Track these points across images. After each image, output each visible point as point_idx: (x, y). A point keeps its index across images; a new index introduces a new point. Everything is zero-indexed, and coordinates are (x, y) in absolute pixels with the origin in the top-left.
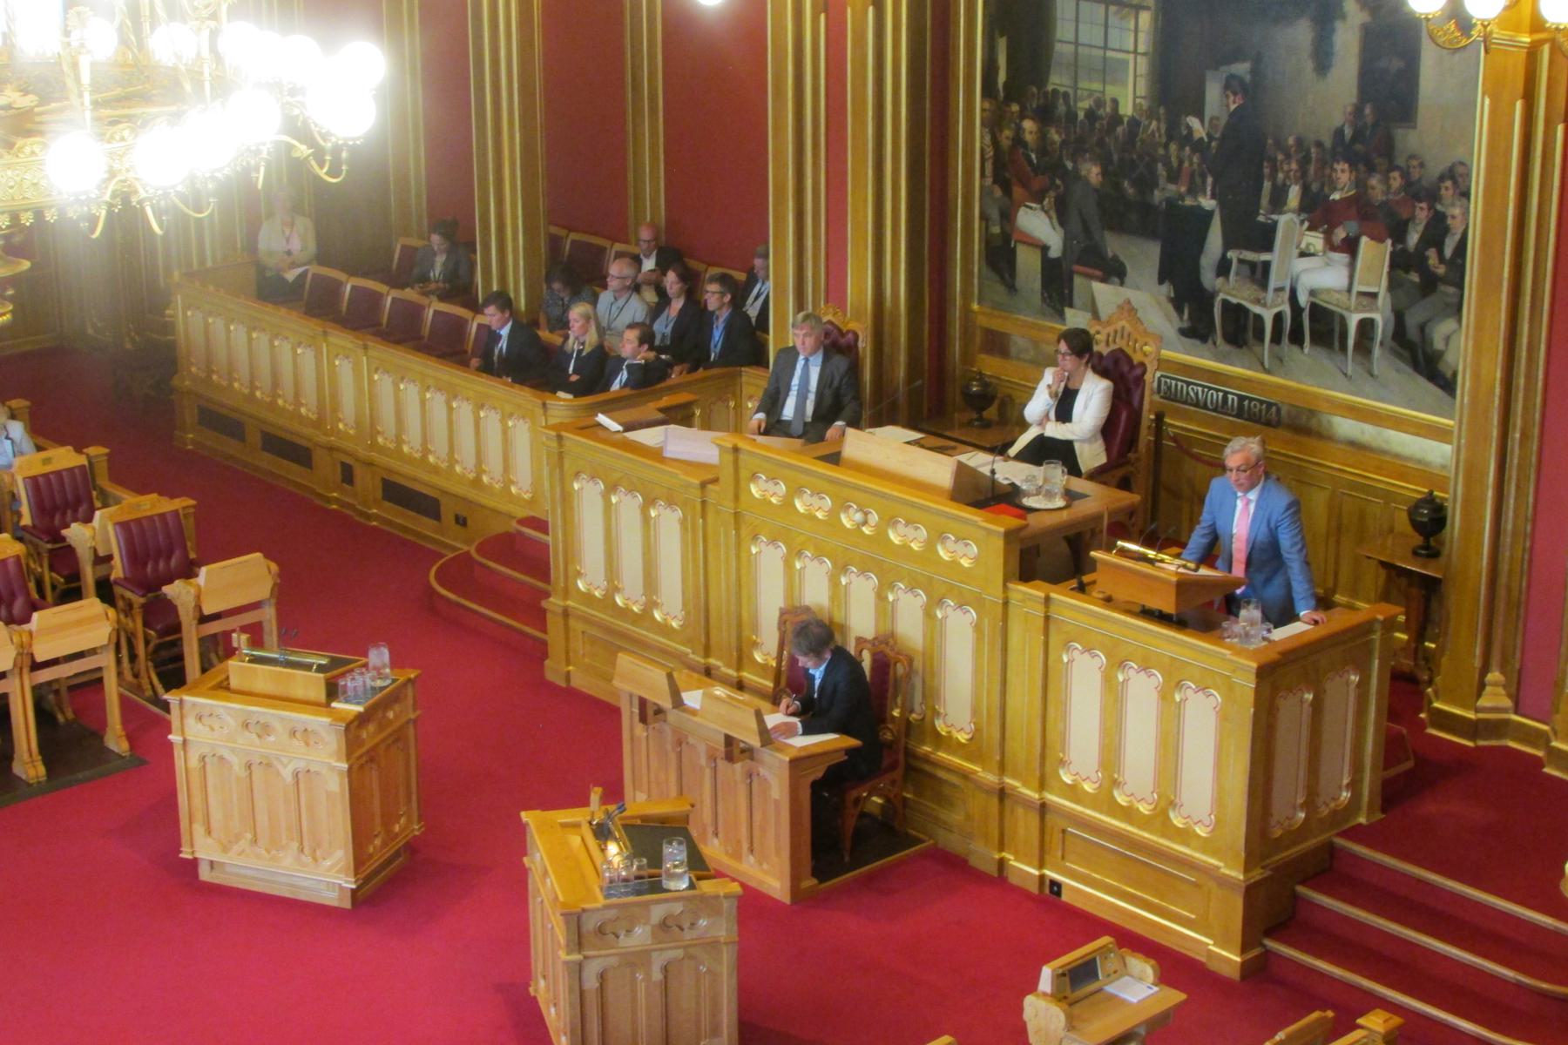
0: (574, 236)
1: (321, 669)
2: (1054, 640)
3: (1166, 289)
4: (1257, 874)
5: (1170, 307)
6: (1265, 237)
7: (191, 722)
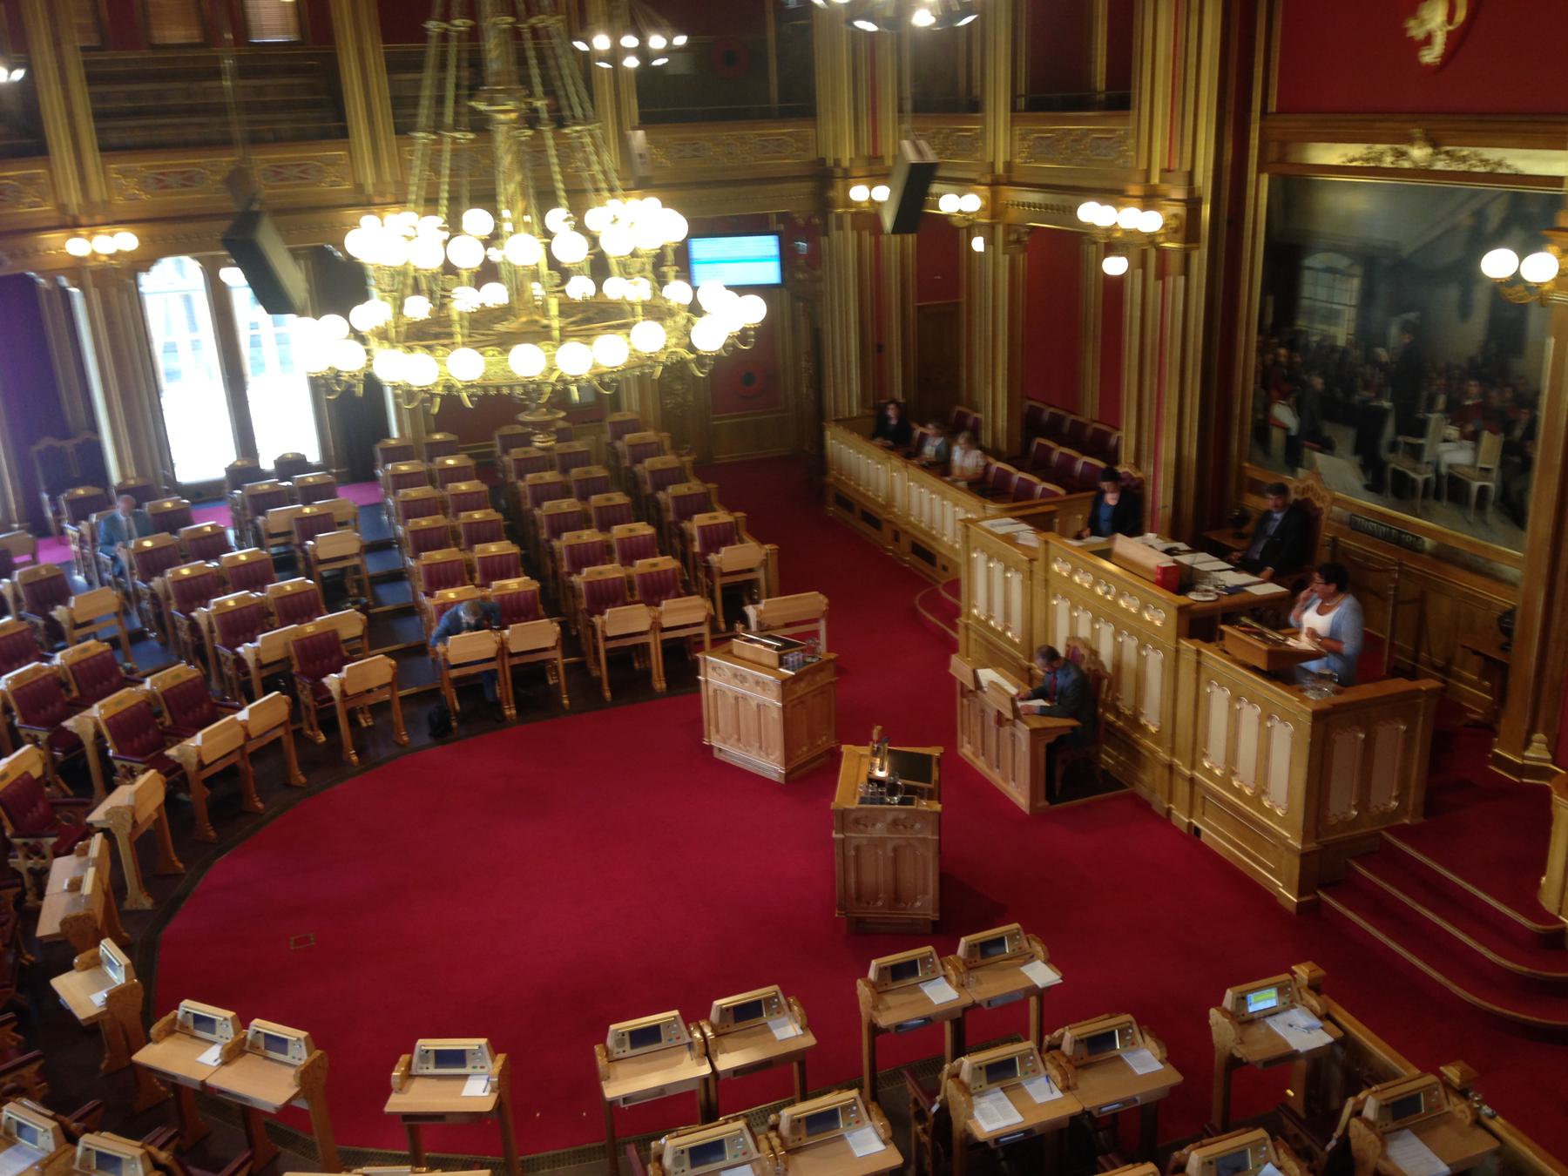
0: (1052, 410)
1: (778, 649)
2: (1203, 677)
3: (1357, 459)
4: (1312, 846)
6: (1420, 429)
7: (709, 670)
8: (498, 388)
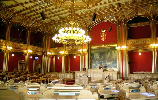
6: (105, 63)
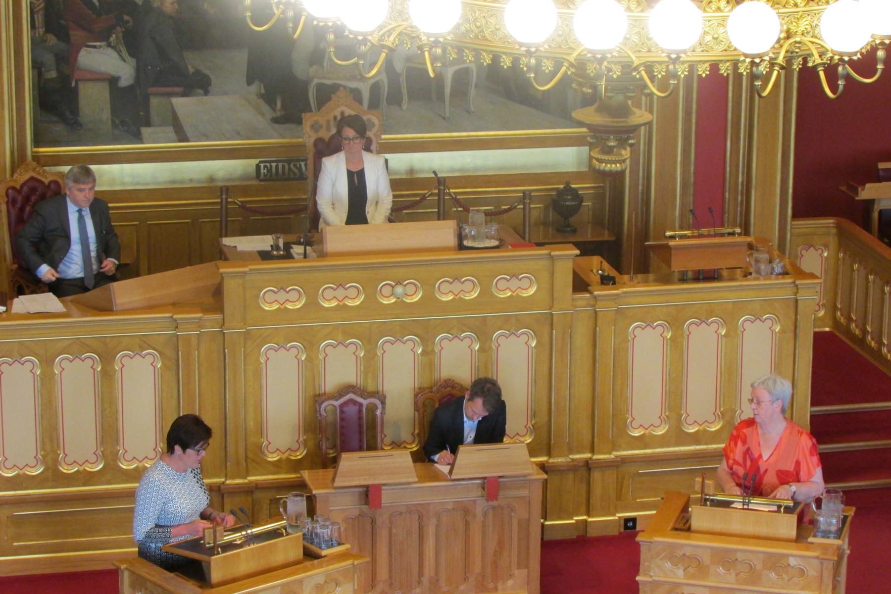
5: (262, 102)
8: (692, 67)
